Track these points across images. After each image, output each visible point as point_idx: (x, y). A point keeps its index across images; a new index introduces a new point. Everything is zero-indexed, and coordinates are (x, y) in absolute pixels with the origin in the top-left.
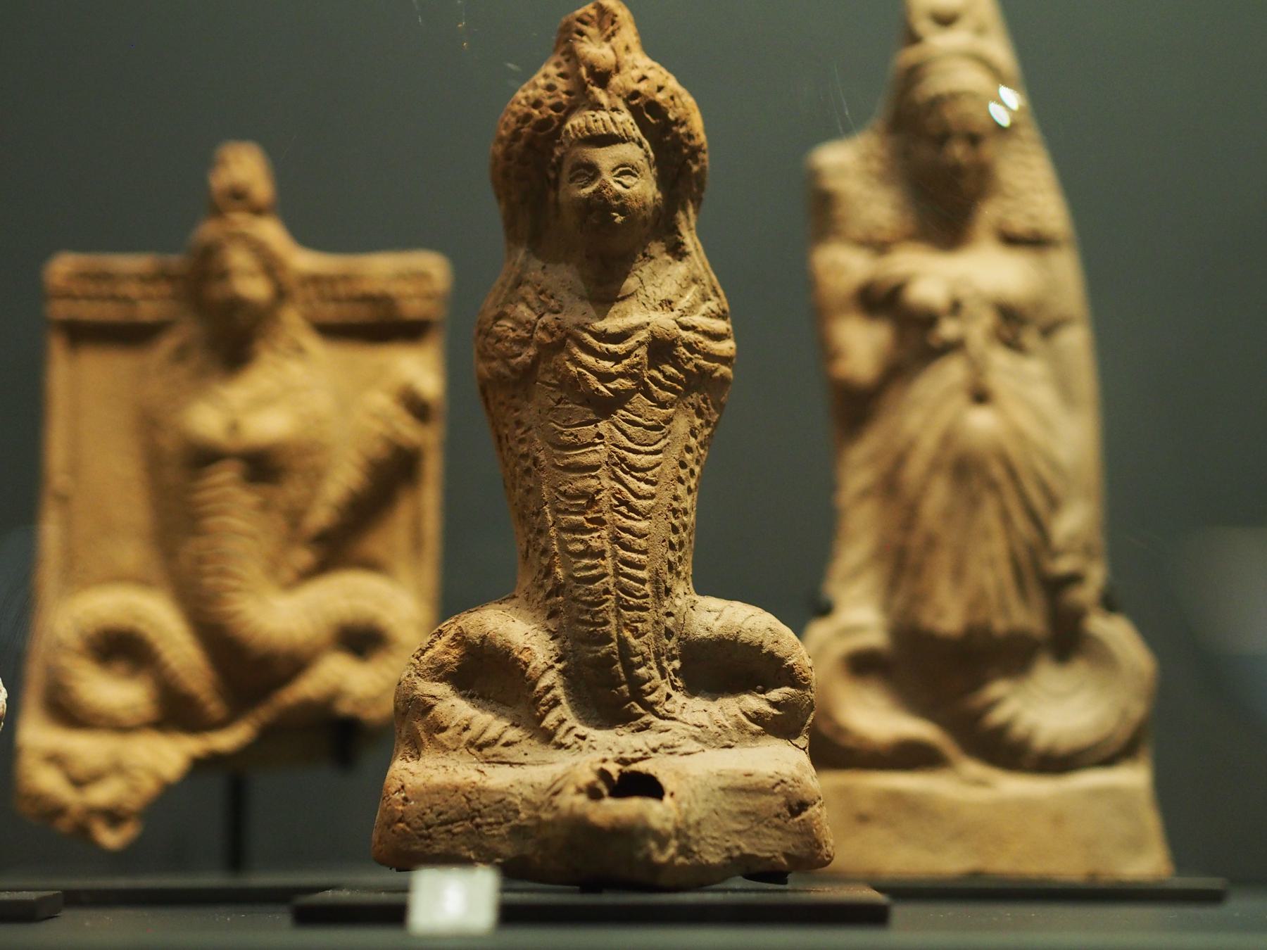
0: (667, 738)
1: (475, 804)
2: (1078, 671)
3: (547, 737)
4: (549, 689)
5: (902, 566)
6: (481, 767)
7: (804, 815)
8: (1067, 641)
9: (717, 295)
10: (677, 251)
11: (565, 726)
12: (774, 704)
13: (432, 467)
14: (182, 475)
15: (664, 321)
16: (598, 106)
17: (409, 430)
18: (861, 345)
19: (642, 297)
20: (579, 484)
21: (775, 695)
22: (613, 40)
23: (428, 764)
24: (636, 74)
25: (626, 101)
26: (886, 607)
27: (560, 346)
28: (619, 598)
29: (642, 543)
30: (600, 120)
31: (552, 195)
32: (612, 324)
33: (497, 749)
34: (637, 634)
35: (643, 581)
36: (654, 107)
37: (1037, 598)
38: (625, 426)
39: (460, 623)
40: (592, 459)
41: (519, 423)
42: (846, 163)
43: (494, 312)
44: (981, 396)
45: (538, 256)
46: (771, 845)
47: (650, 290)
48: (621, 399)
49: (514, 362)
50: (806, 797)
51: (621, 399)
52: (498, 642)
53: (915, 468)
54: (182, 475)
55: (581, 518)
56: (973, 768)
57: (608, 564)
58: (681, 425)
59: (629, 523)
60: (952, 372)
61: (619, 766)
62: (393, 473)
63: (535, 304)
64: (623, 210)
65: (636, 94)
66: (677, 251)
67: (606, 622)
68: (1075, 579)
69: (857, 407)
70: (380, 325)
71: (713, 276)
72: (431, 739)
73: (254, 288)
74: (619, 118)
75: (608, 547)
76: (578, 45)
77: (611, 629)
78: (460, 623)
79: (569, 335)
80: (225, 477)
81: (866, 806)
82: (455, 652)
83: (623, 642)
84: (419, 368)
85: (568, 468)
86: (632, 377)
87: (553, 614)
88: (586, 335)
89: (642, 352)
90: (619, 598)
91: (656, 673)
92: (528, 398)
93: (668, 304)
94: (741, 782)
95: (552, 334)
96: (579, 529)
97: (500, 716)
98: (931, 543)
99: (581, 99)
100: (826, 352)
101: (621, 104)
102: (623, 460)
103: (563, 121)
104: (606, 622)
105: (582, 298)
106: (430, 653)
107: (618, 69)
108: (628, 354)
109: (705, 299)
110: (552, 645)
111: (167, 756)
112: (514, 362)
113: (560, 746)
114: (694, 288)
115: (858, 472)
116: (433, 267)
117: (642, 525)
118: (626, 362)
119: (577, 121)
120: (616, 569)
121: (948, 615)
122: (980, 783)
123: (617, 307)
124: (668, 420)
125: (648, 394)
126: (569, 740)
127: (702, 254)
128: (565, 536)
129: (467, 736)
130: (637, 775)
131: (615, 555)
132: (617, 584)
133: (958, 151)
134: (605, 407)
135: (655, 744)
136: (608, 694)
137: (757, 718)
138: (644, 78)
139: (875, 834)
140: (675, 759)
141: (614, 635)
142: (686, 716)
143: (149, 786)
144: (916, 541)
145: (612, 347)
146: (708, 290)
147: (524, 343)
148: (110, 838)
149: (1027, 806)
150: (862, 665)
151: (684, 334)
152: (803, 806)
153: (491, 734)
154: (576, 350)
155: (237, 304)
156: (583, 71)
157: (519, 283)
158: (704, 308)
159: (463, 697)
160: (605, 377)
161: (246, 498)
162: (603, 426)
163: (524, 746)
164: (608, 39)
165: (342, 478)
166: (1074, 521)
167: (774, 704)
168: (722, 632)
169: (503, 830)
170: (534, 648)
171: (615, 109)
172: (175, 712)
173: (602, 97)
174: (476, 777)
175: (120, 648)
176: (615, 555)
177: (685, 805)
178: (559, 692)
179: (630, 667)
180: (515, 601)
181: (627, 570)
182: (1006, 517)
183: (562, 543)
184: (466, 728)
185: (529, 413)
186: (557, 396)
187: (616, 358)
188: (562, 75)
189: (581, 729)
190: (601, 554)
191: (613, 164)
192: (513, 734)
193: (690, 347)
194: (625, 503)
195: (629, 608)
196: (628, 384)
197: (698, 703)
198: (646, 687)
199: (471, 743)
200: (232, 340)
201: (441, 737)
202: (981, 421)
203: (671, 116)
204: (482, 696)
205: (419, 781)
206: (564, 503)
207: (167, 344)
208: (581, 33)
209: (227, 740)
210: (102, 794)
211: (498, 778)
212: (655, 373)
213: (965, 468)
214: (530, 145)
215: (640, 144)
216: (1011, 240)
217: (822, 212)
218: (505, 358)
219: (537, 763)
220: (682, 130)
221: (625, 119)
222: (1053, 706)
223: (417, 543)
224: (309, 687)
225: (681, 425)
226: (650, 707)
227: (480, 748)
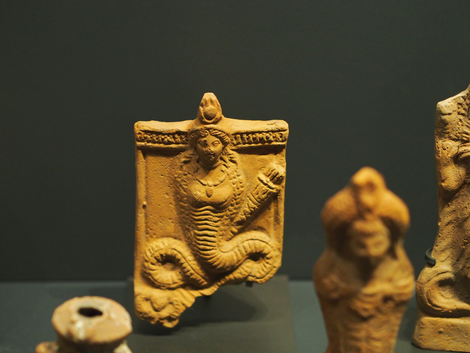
13: (283, 195)
14: (190, 212)
26: (453, 265)
48: (371, 317)
54: (190, 212)
69: (449, 196)
81: (441, 330)
84: (277, 164)
111: (187, 298)
115: (446, 216)
134: (364, 319)
143: (182, 309)
148: (168, 325)
150: (443, 284)
155: (209, 154)
160: (366, 310)
165: (248, 205)
172: (189, 283)
175: (168, 260)
200: (207, 163)
207: (182, 158)
209: (207, 292)
210: (164, 313)
217: (441, 127)
223: (277, 220)
224: (236, 274)
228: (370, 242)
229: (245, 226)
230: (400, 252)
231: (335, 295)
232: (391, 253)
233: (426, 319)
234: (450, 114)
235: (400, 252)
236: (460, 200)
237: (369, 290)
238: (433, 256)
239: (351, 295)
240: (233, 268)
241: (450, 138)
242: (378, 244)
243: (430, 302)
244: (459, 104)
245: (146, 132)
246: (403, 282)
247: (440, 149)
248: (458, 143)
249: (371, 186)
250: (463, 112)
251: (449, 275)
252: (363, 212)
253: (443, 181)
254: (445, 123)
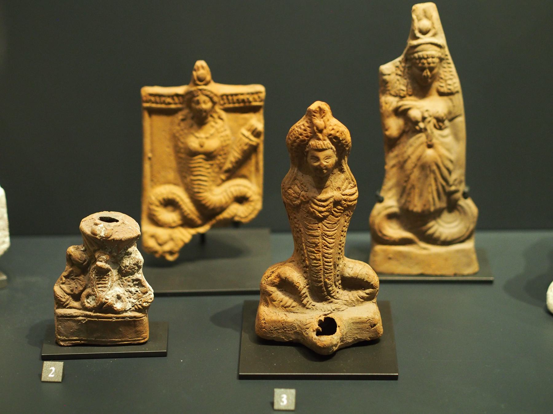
0: (337, 306)
1: (284, 325)
2: (455, 214)
3: (304, 306)
4: (304, 293)
5: (404, 191)
6: (286, 313)
7: (375, 327)
8: (452, 206)
9: (353, 181)
10: (342, 171)
11: (309, 303)
12: (367, 294)
13: (261, 148)
15: (337, 195)
16: (319, 139)
17: (254, 140)
18: (394, 126)
19: (331, 186)
20: (313, 240)
21: (368, 291)
22: (324, 118)
23: (271, 311)
24: (331, 128)
25: (328, 137)
26: (399, 201)
27: (308, 202)
28: (324, 271)
29: (331, 256)
30: (320, 144)
31: (305, 158)
32: (322, 196)
33: (290, 308)
34: (329, 279)
35: (331, 266)
36: (336, 138)
37: (444, 198)
38: (326, 224)
39: (279, 271)
40: (317, 234)
41: (295, 218)
42: (390, 69)
43: (288, 186)
44: (430, 146)
45: (300, 171)
46: (366, 336)
47: (334, 183)
48: (325, 217)
49: (294, 203)
50: (376, 323)
51: (325, 217)
52: (290, 280)
53: (409, 165)
55: (313, 249)
56: (423, 245)
57: (321, 262)
58: (342, 221)
59: (327, 251)
60: (422, 137)
61: (324, 317)
62: (249, 152)
63: (300, 187)
64: (326, 169)
65: (331, 135)
66: (342, 171)
67: (321, 278)
68: (456, 191)
69: (393, 143)
70: (245, 108)
71: (353, 176)
72: (271, 303)
73: (207, 106)
74: (325, 142)
75: (321, 258)
76: (314, 120)
77: (322, 279)
78: (279, 271)
79: (310, 200)
80: (199, 159)
81: (391, 256)
82: (278, 279)
83: (325, 282)
84: (257, 121)
85: (310, 235)
86: (328, 211)
87: (305, 272)
88: (315, 200)
89: (332, 205)
90: (324, 271)
91: (334, 287)
92: (298, 212)
93: (339, 188)
94: (358, 321)
95: (305, 199)
96: (313, 252)
97: (290, 298)
98: (413, 187)
99: (314, 135)
100: (383, 127)
101: (326, 138)
102: (326, 234)
103: (309, 141)
104: (321, 278)
105: (314, 187)
106: (270, 278)
107: (325, 128)
108: (327, 206)
109: (350, 183)
110: (305, 281)
111: (185, 235)
112: (294, 203)
113: (308, 308)
114: (347, 181)
115: (391, 160)
116: (260, 88)
117: (331, 251)
118: (327, 208)
119: (313, 142)
120: (323, 264)
121: (417, 206)
122: (425, 249)
123: (324, 190)
124: (338, 221)
125: (333, 215)
126: (310, 307)
127: (349, 170)
128: (309, 253)
129: (282, 304)
130: (329, 318)
131: (323, 260)
132: (324, 268)
133: (427, 73)
134: (321, 220)
135: (334, 308)
136: (321, 294)
137: (362, 298)
138: (333, 129)
139: (393, 262)
140: (340, 313)
141: (323, 280)
142: (342, 298)
143: (181, 244)
144: (409, 186)
145: (323, 204)
146: (351, 181)
147: (297, 198)
148: (170, 258)
149: (438, 255)
150: (391, 217)
151: (344, 197)
152: (375, 325)
153: (288, 304)
154: (312, 204)
155: (201, 111)
156: (315, 128)
157: (295, 179)
158: (349, 186)
159: (280, 291)
160: (321, 212)
161: (206, 165)
162: (320, 225)
163: (297, 307)
164: (322, 118)
165: (234, 155)
166: (457, 175)
167: (367, 294)
168: (353, 275)
169: (292, 332)
170: (300, 282)
171: (325, 140)
172: (187, 223)
173: (320, 136)
174: (284, 318)
175: (170, 203)
176: (323, 260)
177: (342, 331)
178: (307, 294)
179: (327, 288)
180: (294, 263)
181: (327, 264)
182: (436, 180)
183: (308, 255)
184: (281, 302)
185: (298, 216)
186: (307, 215)
187: (324, 207)
188: (308, 127)
189: (314, 303)
190: (320, 260)
191: (324, 157)
192: (294, 304)
193: (345, 200)
194: (326, 246)
195: (327, 273)
196: (327, 213)
197: (346, 292)
198: (331, 292)
199: (282, 306)
200: (200, 119)
201: (274, 303)
202: (430, 152)
203: (341, 139)
204: (285, 291)
205: (269, 318)
206: (309, 244)
207: (180, 116)
208: (314, 116)
209: (202, 230)
210: (167, 247)
211: (291, 318)
212: (335, 209)
213: (424, 167)
214: (299, 145)
215: (332, 149)
216: (441, 94)
217: (383, 86)
218: (291, 200)
219: (301, 313)
220: (344, 142)
221: (328, 143)
222: (447, 226)
223: (257, 169)
224: (225, 215)
225: (342, 221)
226: (332, 297)
227: (285, 308)
228: (321, 155)
229: (233, 173)
230: (346, 167)
231: (298, 202)
232: (338, 166)
233: (379, 248)
234: (389, 75)
235: (346, 167)
236: (401, 146)
237: (322, 196)
238: (382, 194)
239: (308, 201)
240: (222, 209)
241: (391, 95)
242: (328, 157)
243: (381, 232)
244: (397, 67)
245: (151, 95)
246: (348, 191)
247: (383, 104)
248: (397, 99)
249: (321, 111)
250: (399, 73)
251: (395, 209)
252: (316, 132)
253: (387, 130)
254: (386, 82)
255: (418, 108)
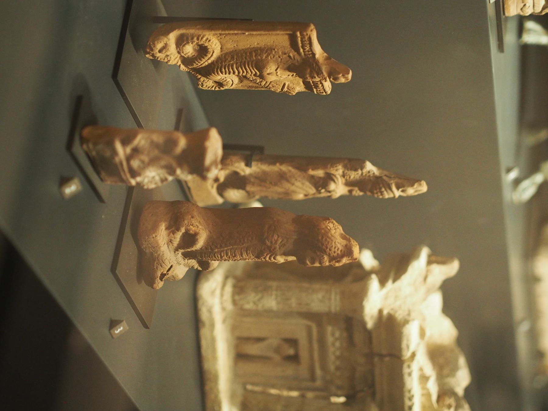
27: (270, 251)
52: (197, 243)
53: (287, 185)
87: (206, 248)
103: (326, 254)
122: (212, 187)
128: (225, 252)
129: (173, 239)
147: (271, 242)
201: (172, 234)
205: (159, 239)
206: (233, 251)
231: (268, 243)
238: (254, 163)
245: (310, 39)
255: (336, 187)
